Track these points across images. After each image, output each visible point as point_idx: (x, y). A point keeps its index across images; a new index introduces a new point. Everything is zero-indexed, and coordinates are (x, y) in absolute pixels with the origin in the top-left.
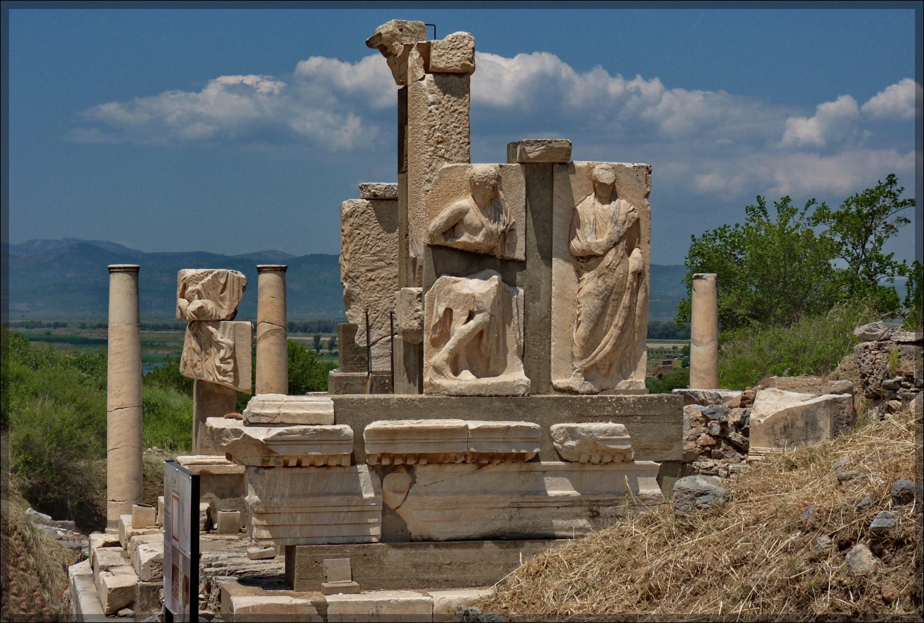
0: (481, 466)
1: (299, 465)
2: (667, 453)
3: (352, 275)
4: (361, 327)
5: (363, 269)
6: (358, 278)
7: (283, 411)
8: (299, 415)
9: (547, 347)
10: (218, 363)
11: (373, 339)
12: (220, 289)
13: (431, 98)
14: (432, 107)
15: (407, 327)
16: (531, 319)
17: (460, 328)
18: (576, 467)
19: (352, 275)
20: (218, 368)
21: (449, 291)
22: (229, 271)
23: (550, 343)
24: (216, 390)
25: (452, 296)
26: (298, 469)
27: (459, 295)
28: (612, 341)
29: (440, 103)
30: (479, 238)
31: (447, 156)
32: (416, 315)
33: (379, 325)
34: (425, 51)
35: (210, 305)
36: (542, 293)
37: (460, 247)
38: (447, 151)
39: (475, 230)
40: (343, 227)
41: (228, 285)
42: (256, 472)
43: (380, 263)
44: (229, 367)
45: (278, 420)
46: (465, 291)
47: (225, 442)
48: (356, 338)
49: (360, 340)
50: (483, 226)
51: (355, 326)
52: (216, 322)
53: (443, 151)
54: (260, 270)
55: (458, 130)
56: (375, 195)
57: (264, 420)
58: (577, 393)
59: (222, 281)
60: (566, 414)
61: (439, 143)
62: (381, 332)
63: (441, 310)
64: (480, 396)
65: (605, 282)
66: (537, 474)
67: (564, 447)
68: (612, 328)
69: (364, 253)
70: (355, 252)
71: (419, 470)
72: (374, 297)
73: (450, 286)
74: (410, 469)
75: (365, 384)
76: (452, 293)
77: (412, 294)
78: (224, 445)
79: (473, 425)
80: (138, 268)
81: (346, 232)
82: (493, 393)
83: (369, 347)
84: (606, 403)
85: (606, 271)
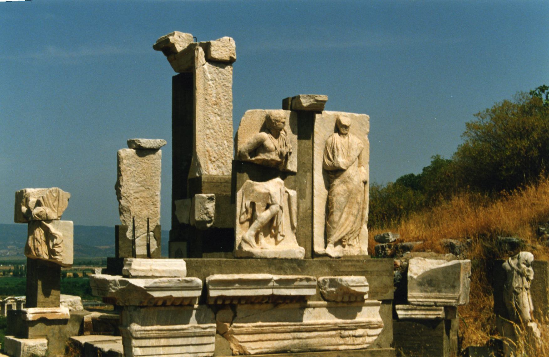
2: (385, 295)
4: (130, 228)
6: (128, 197)
7: (154, 267)
8: (164, 271)
14: (210, 82)
15: (200, 219)
18: (333, 305)
19: (125, 195)
22: (60, 190)
26: (163, 308)
27: (260, 193)
28: (351, 224)
29: (215, 80)
30: (274, 156)
31: (219, 113)
32: (205, 212)
34: (207, 48)
39: (269, 151)
42: (135, 310)
46: (263, 190)
49: (129, 235)
50: (276, 149)
55: (226, 97)
56: (140, 146)
58: (330, 257)
60: (327, 270)
61: (214, 105)
62: (141, 230)
63: (248, 203)
67: (327, 292)
74: (233, 307)
76: (255, 192)
77: (203, 198)
78: (113, 291)
79: (276, 277)
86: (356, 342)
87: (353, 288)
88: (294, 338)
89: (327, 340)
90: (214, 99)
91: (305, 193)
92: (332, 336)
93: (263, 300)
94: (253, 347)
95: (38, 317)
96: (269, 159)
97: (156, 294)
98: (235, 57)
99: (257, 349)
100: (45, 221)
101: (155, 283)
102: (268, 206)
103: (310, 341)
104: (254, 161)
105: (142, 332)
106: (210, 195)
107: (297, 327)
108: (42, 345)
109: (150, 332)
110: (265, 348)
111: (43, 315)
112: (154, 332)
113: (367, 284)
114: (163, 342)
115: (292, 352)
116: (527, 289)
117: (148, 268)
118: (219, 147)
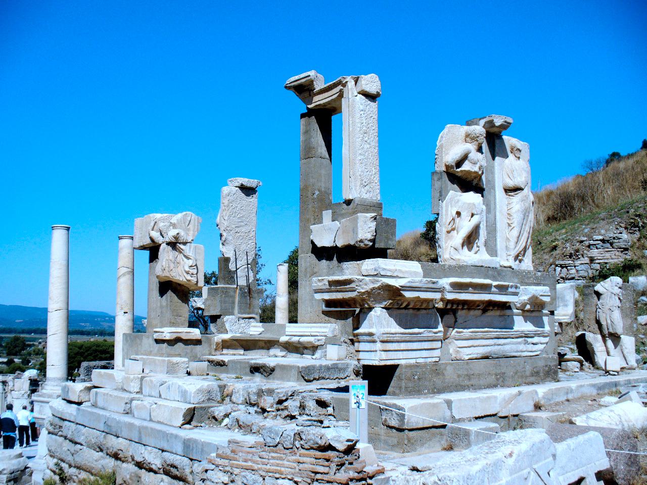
0: (485, 311)
1: (406, 308)
2: (551, 306)
3: (228, 229)
4: (233, 259)
5: (234, 226)
7: (398, 268)
9: (495, 243)
10: (187, 269)
11: (238, 267)
12: (187, 224)
13: (362, 107)
14: (362, 112)
16: (488, 224)
17: (465, 226)
19: (228, 229)
20: (188, 273)
21: (458, 201)
23: (496, 239)
24: (179, 288)
25: (460, 204)
33: (241, 259)
35: (182, 233)
36: (492, 208)
37: (459, 175)
38: (369, 139)
40: (224, 201)
41: (192, 222)
43: (242, 224)
44: (195, 271)
45: (395, 274)
47: (362, 288)
48: (230, 265)
49: (232, 267)
51: (227, 260)
52: (185, 244)
53: (367, 138)
54: (120, 238)
55: (373, 128)
56: (242, 185)
57: (389, 274)
59: (189, 219)
64: (482, 266)
65: (525, 205)
66: (506, 317)
68: (525, 232)
69: (234, 217)
70: (230, 216)
71: (460, 313)
72: (239, 242)
73: (458, 198)
74: (454, 312)
75: (235, 292)
76: (460, 202)
80: (69, 228)
81: (226, 204)
82: (487, 266)
83: (236, 271)
84: (530, 276)
85: (525, 198)
86: (534, 350)
87: (541, 298)
88: (495, 345)
89: (514, 347)
90: (364, 128)
91: (490, 207)
92: (520, 343)
93: (478, 306)
94: (468, 353)
95: (174, 336)
96: (473, 171)
97: (408, 295)
98: (381, 93)
99: (470, 354)
100: (180, 243)
101: (409, 282)
102: (472, 215)
103: (507, 348)
104: (458, 172)
105: (388, 335)
106: (373, 215)
107: (498, 333)
108: (183, 362)
109: (394, 336)
110: (475, 354)
111: (179, 335)
112: (397, 335)
113: (550, 294)
114: (403, 346)
115: (493, 358)
116: (619, 307)
117: (392, 268)
118: (368, 173)
